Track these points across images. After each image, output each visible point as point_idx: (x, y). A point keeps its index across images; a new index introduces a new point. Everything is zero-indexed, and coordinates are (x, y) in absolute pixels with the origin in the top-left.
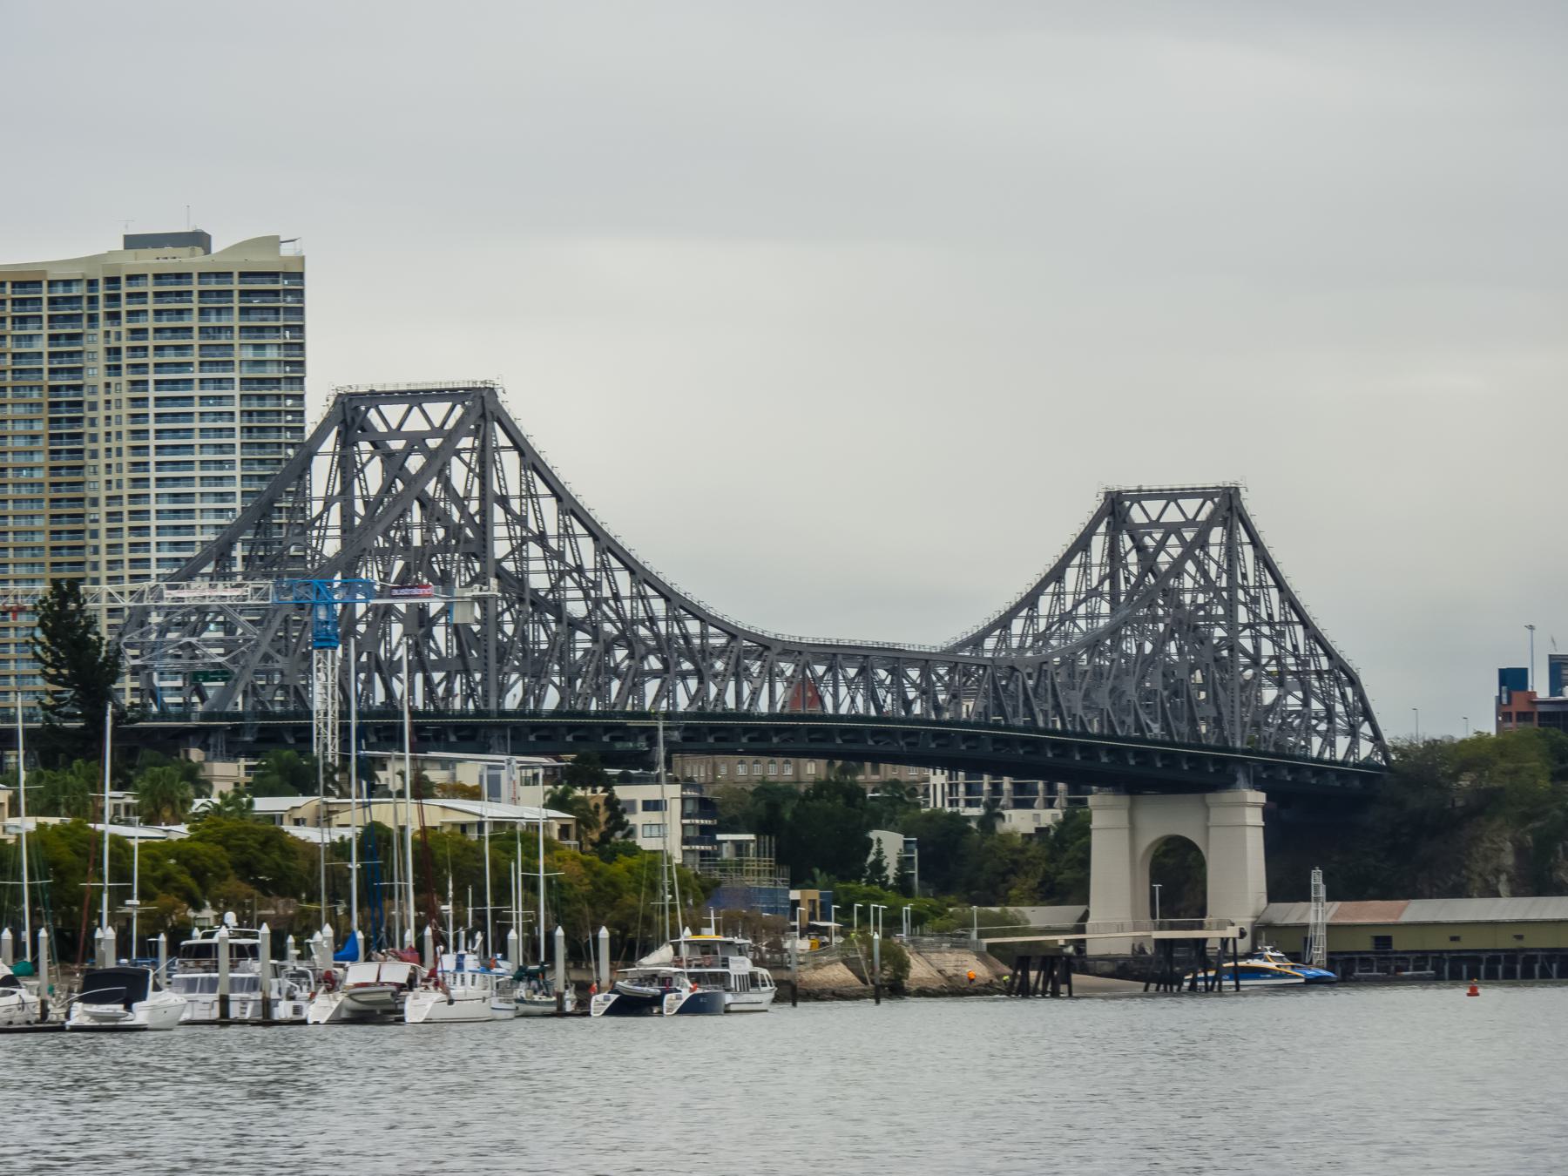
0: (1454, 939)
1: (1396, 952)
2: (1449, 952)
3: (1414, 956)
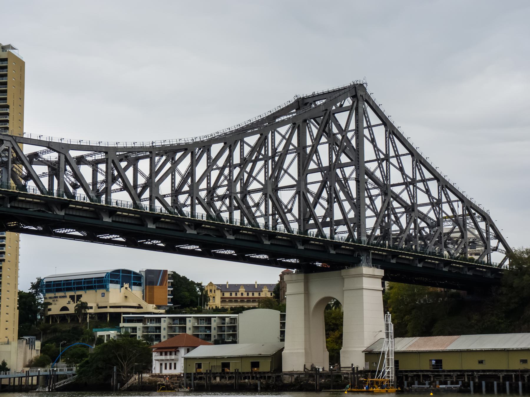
0: (481, 362)
1: (444, 371)
2: (478, 371)
3: (456, 374)
